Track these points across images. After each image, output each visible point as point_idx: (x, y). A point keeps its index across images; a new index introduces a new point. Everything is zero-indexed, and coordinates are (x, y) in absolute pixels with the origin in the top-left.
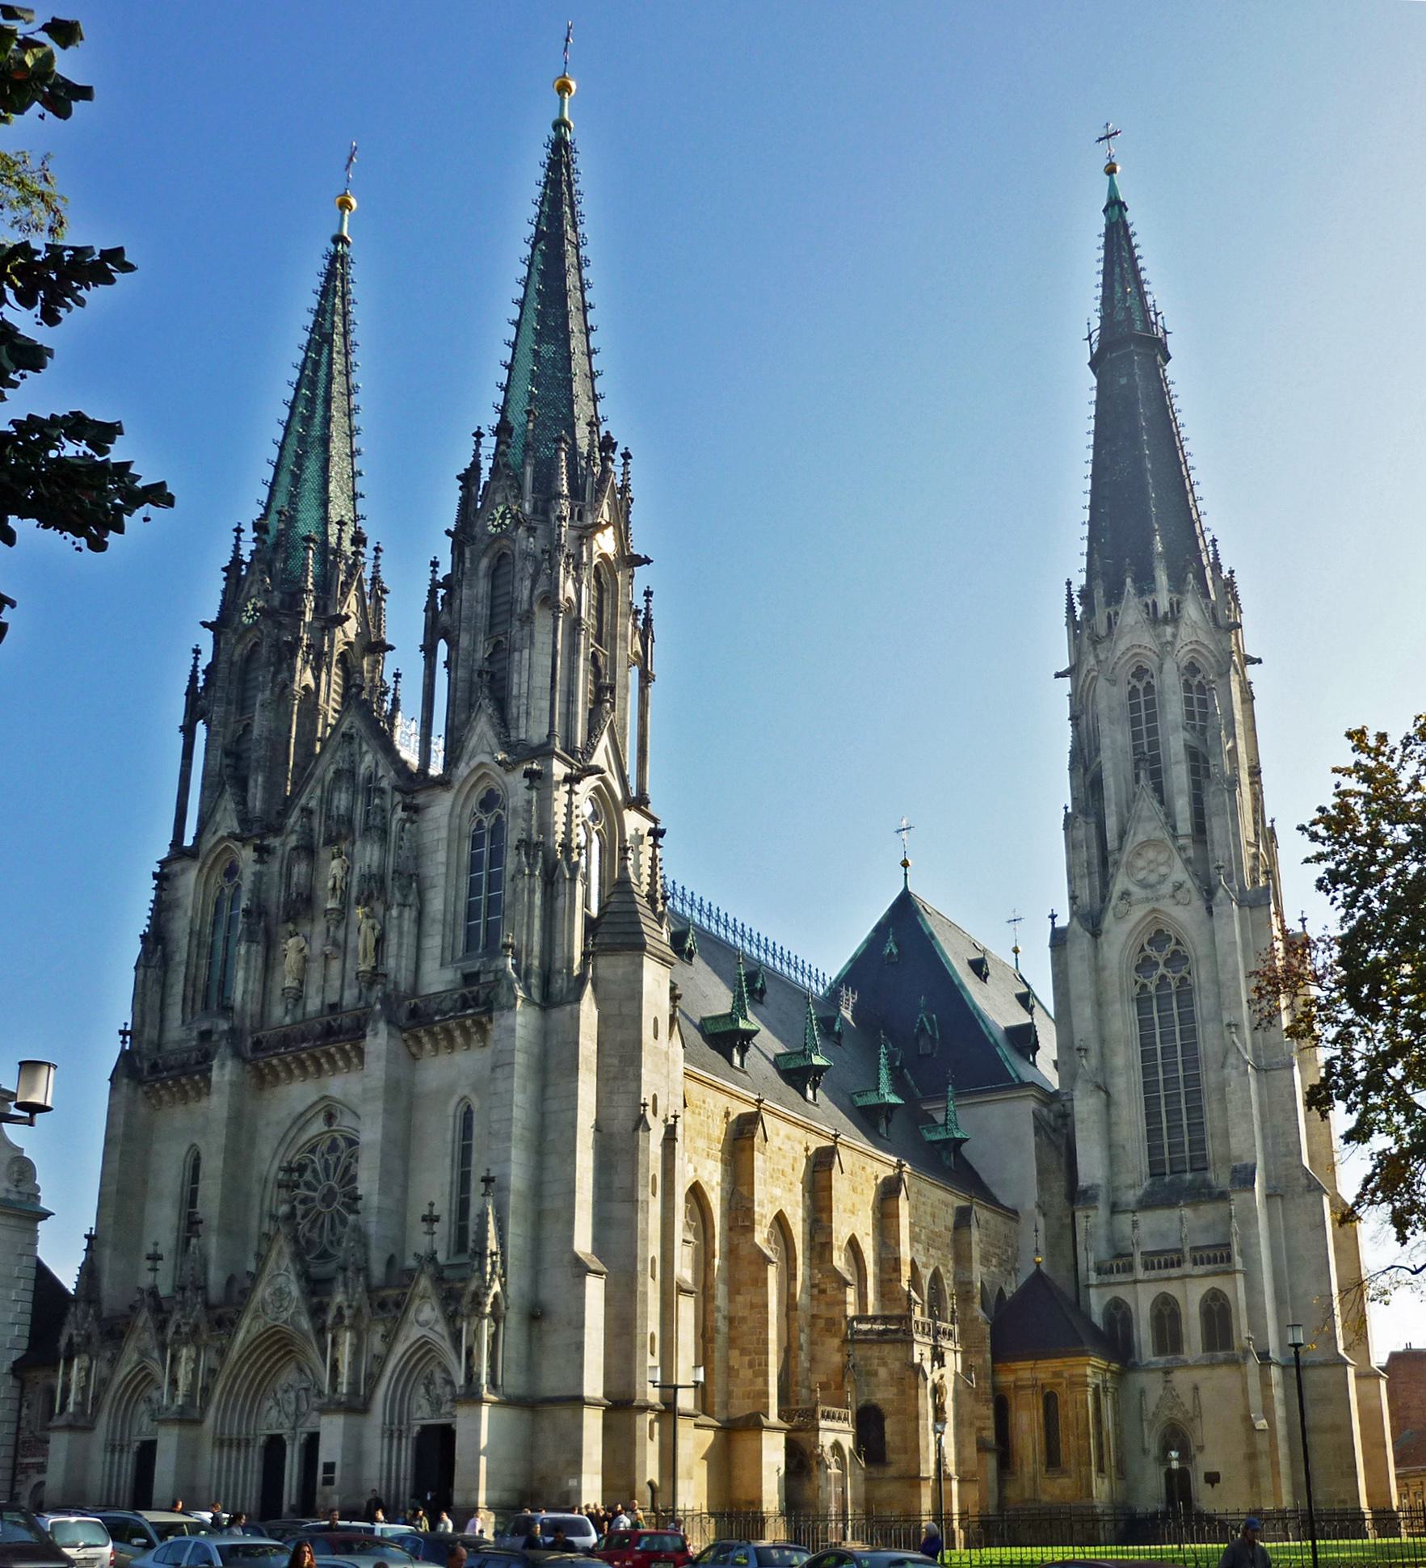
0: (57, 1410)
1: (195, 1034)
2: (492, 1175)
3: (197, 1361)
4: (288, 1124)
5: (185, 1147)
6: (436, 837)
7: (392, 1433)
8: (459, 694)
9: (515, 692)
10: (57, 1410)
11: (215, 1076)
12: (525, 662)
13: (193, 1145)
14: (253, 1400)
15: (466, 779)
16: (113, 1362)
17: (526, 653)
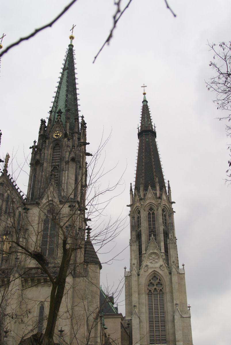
2: (63, 329)
9: (63, 182)
12: (66, 174)
15: (44, 204)
17: (67, 172)
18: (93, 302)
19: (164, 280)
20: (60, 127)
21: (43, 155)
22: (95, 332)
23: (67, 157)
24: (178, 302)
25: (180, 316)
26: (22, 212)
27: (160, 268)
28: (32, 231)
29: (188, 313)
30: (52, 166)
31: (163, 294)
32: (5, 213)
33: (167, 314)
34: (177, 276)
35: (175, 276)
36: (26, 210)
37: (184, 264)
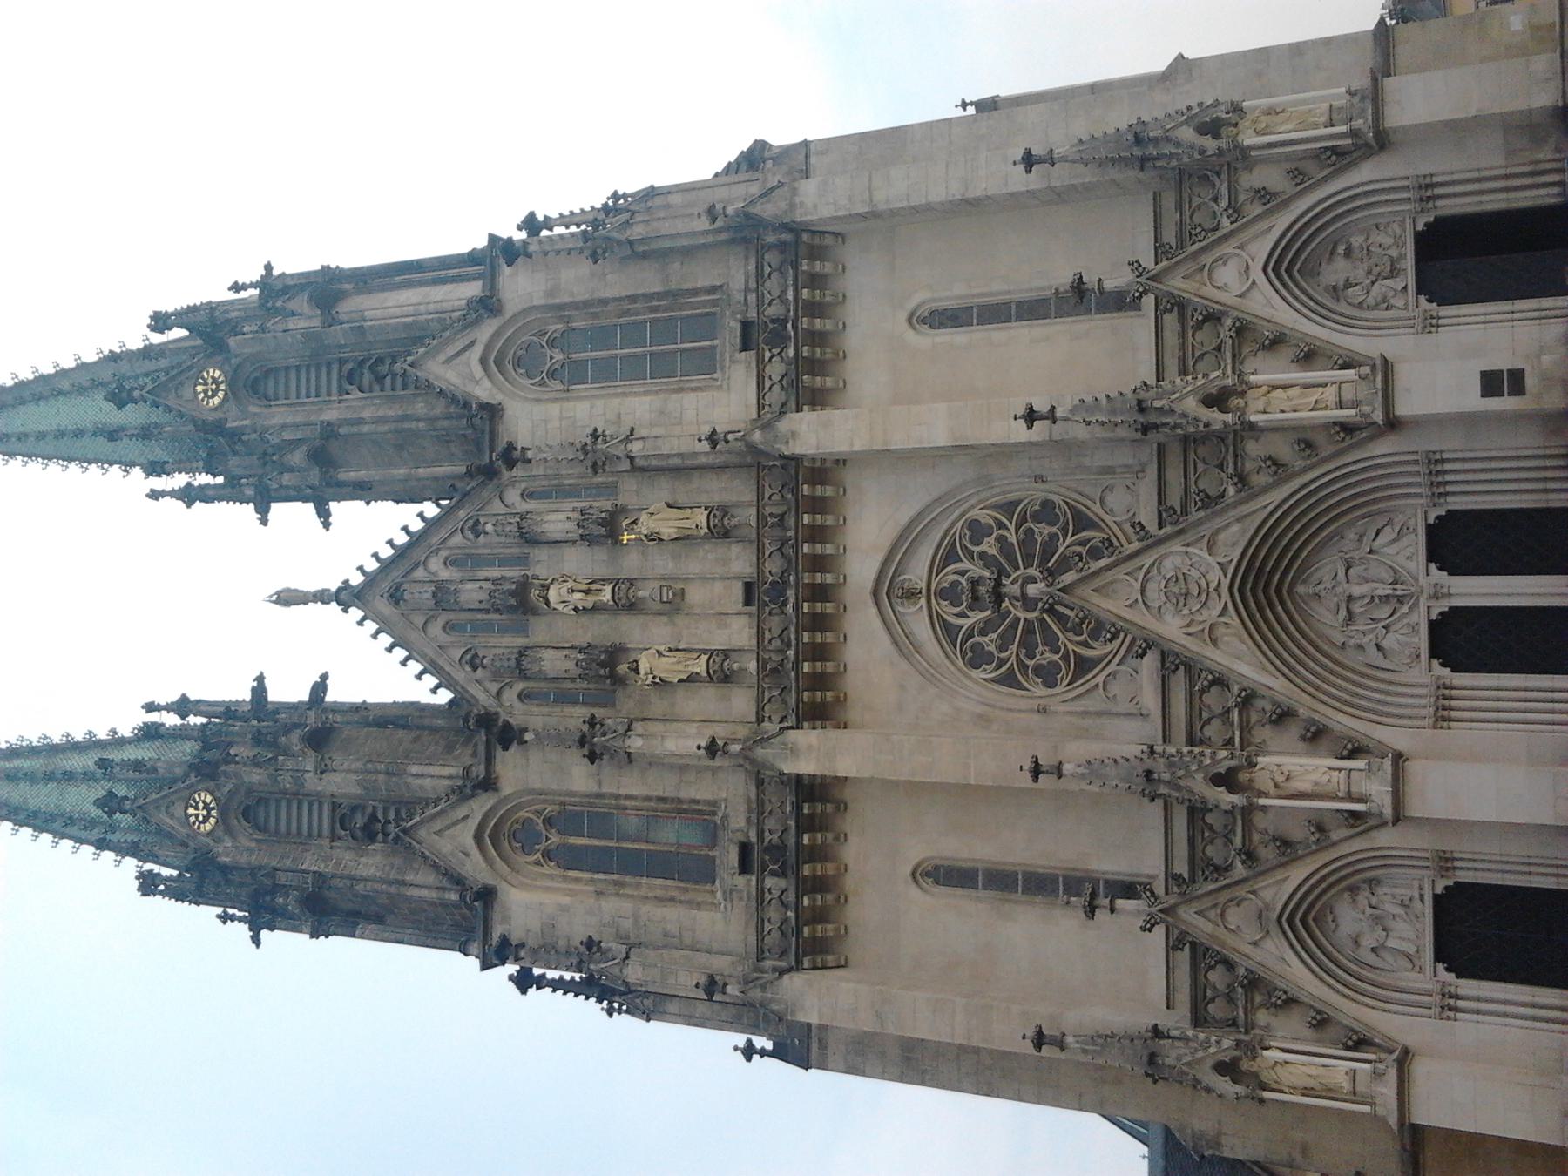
0: (1366, 1109)
1: (740, 881)
4: (904, 665)
5: (914, 891)
6: (557, 424)
8: (391, 413)
10: (1366, 1109)
11: (806, 766)
13: (913, 874)
14: (1363, 675)
17: (368, 314)
20: (176, 382)
21: (287, 436)
23: (306, 325)
26: (523, 485)
28: (606, 422)
30: (342, 392)
32: (523, 561)
36: (511, 457)
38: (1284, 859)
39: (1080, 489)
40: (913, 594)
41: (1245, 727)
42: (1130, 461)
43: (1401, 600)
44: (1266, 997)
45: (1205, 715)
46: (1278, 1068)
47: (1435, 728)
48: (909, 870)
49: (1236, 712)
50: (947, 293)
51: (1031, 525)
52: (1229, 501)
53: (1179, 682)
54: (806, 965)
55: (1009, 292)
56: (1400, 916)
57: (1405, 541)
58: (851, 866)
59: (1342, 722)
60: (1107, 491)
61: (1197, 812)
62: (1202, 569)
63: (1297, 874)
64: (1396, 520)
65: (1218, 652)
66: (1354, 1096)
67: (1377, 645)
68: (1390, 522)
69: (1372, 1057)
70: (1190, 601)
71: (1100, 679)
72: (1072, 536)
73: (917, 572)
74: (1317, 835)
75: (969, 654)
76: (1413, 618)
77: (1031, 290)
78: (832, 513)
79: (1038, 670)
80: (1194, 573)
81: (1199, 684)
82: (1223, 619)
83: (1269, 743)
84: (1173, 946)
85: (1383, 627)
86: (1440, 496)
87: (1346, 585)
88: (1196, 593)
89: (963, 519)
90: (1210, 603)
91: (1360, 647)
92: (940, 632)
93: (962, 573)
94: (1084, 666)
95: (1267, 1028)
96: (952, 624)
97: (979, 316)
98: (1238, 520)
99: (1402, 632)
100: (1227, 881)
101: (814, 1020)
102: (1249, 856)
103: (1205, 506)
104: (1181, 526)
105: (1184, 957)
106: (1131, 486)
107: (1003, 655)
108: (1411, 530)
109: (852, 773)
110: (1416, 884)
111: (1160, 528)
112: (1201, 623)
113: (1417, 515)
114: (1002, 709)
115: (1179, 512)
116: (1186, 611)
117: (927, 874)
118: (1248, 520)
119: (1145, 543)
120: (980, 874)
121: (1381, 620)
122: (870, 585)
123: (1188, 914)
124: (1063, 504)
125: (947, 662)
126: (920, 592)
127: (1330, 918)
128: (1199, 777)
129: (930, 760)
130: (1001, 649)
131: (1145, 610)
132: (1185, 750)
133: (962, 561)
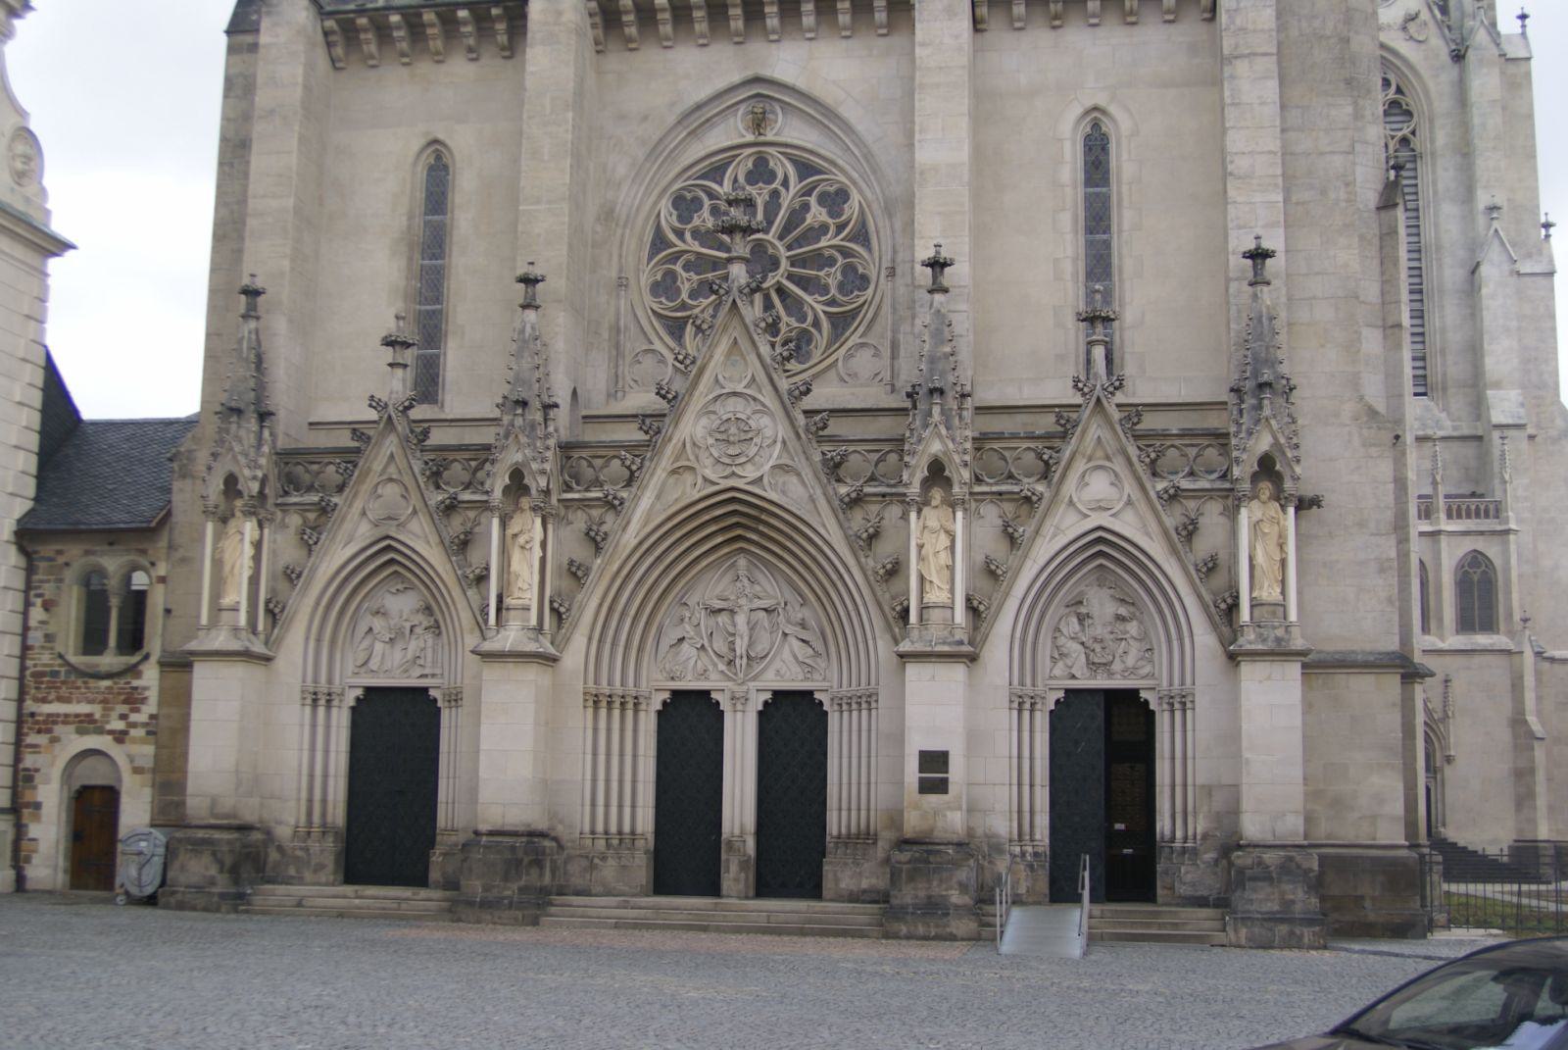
0: (204, 620)
3: (544, 545)
4: (672, 119)
5: (417, 144)
7: (1023, 703)
10: (204, 620)
13: (436, 141)
16: (310, 540)
18: (1363, 117)
19: (1426, 92)
22: (1383, 273)
24: (1499, 200)
25: (1506, 267)
27: (1404, 29)
29: (1540, 252)
31: (1414, 159)
33: (1439, 260)
34: (1496, 72)
35: (1485, 70)
37: (1526, 11)
38: (447, 543)
39: (879, 319)
40: (759, 125)
41: (585, 504)
42: (903, 377)
43: (730, 663)
44: (311, 524)
45: (598, 462)
46: (239, 537)
47: (585, 694)
48: (441, 136)
49: (600, 495)
50: (1125, 156)
51: (839, 264)
52: (830, 489)
53: (631, 434)
54: (330, 24)
55: (1120, 231)
56: (405, 656)
57: (796, 669)
58: (443, 68)
59: (589, 605)
60: (872, 351)
61: (483, 454)
62: (757, 458)
63: (432, 553)
64: (819, 660)
65: (664, 475)
66: (217, 609)
67: (684, 638)
68: (817, 654)
69: (261, 627)
70: (723, 446)
71: (658, 346)
72: (825, 312)
73: (790, 130)
74: (471, 576)
75: (689, 196)
76: (714, 676)
77: (1120, 259)
78: (818, 23)
79: (671, 275)
80: (753, 450)
81: (628, 456)
82: (700, 481)
83: (569, 528)
84: (357, 430)
85: (703, 646)
86: (846, 703)
87: (746, 608)
88: (731, 451)
89: (848, 183)
90: (720, 467)
91: (682, 620)
92: (714, 159)
93: (785, 183)
94: (676, 328)
95: (284, 526)
96: (724, 173)
97: (1097, 195)
98: (811, 496)
99: (699, 662)
100: (422, 485)
101: (264, 38)
102: (450, 508)
103: (825, 462)
104: (803, 436)
105: (345, 440)
106: (879, 377)
107: (688, 236)
108: (809, 675)
109: (530, 68)
110: (438, 671)
111: (805, 412)
112: (697, 458)
113: (825, 683)
114: (623, 236)
115: (821, 433)
116: (711, 441)
117: (439, 157)
118: (810, 506)
119: (786, 397)
120: (441, 217)
121: (710, 641)
122: (767, 73)
123: (391, 445)
124: (861, 302)
125: (677, 169)
126: (760, 134)
127: (400, 587)
128: (518, 457)
129: (546, 158)
130: (696, 234)
131: (711, 397)
132: (552, 442)
133: (800, 182)
